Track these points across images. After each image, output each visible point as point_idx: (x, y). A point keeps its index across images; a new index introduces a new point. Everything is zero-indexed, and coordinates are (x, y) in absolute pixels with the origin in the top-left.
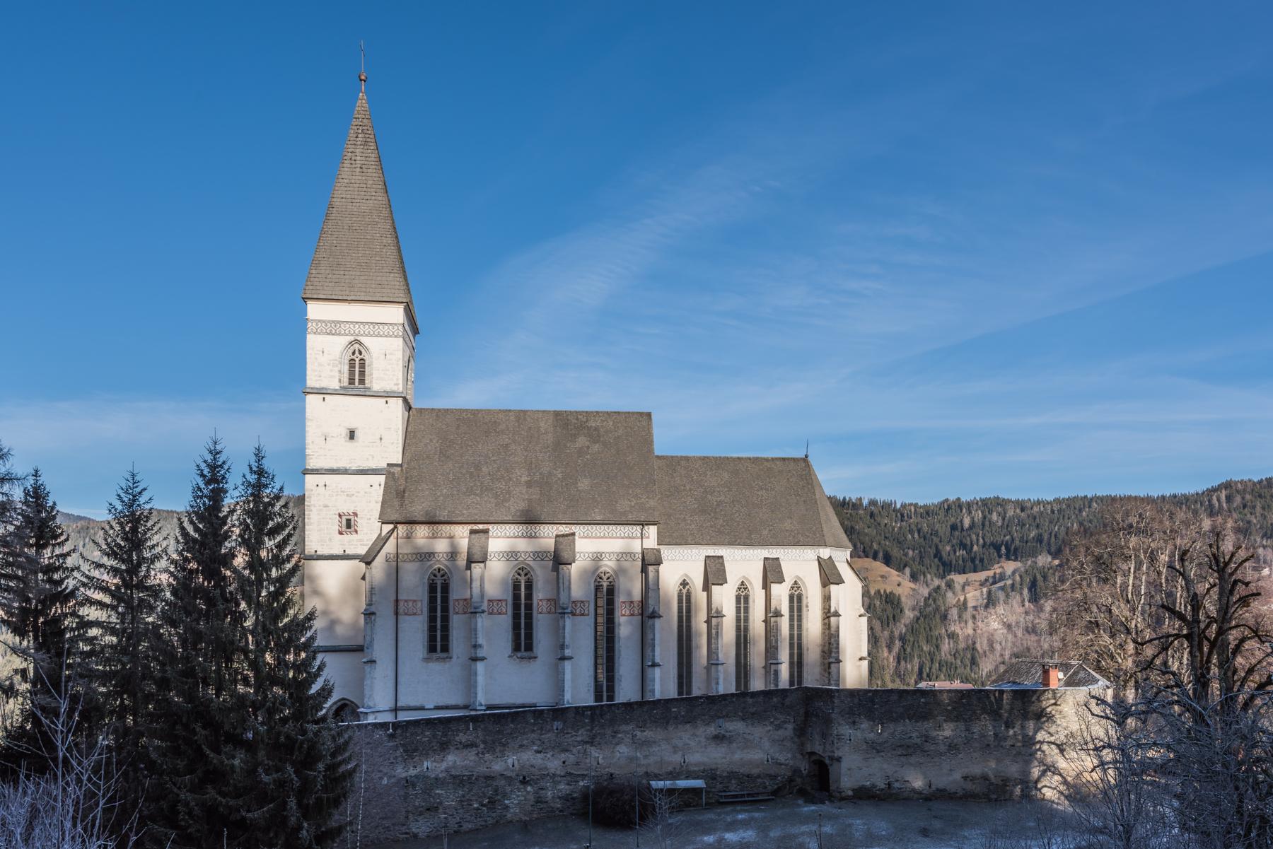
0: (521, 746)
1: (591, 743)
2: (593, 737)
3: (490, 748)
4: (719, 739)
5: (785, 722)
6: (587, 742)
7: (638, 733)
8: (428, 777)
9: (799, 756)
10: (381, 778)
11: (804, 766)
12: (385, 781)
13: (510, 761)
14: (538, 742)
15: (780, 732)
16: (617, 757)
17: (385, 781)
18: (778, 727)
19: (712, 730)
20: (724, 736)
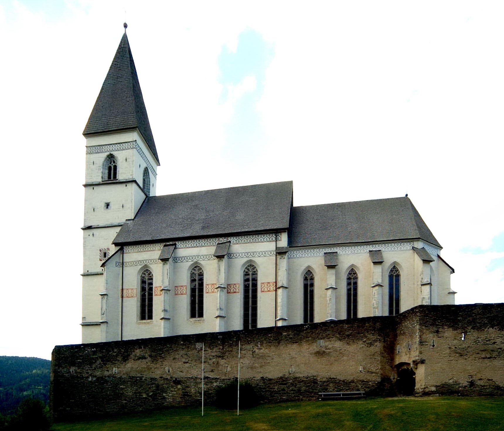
0: (174, 359)
1: (222, 357)
2: (224, 353)
3: (154, 359)
4: (320, 354)
5: (375, 341)
6: (219, 357)
7: (257, 351)
8: (115, 377)
9: (388, 367)
10: (88, 377)
11: (394, 376)
12: (90, 379)
13: (167, 369)
14: (186, 356)
15: (372, 349)
16: (243, 366)
17: (90, 379)
18: (371, 344)
19: (314, 348)
20: (324, 352)
